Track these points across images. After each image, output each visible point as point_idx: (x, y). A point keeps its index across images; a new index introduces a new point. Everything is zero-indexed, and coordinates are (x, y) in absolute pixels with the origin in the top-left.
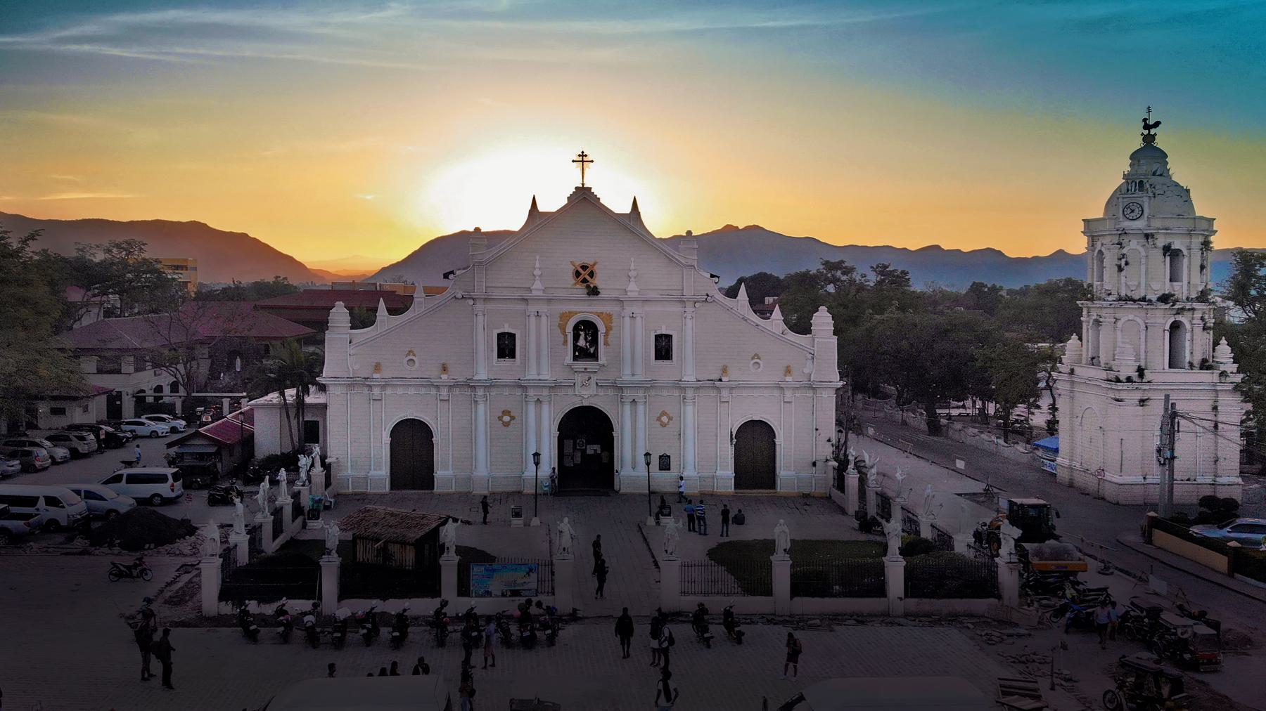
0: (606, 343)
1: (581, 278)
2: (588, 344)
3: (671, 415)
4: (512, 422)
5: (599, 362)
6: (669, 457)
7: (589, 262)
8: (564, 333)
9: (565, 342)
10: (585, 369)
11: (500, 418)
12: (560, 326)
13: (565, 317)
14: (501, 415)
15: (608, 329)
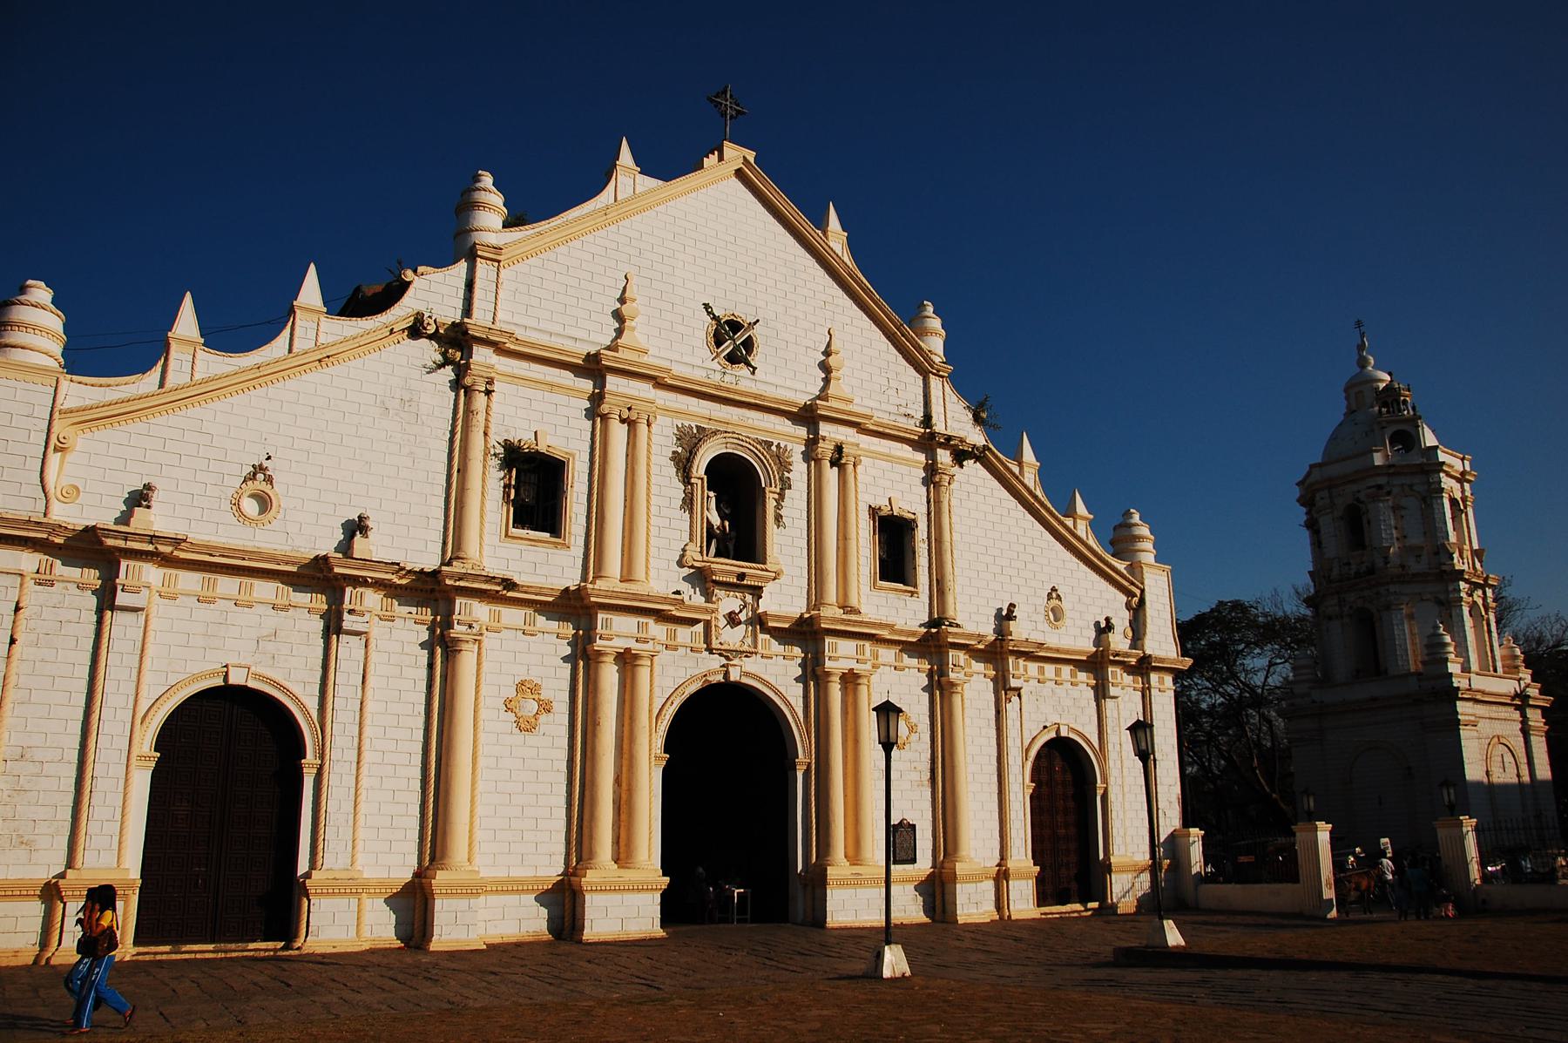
0: (778, 518)
1: (728, 347)
2: (727, 523)
3: (913, 720)
4: (543, 718)
5: (768, 566)
6: (914, 826)
7: (746, 317)
8: (686, 478)
9: (688, 503)
10: (742, 576)
11: (508, 706)
12: (675, 457)
13: (690, 441)
14: (511, 693)
15: (786, 484)
